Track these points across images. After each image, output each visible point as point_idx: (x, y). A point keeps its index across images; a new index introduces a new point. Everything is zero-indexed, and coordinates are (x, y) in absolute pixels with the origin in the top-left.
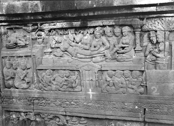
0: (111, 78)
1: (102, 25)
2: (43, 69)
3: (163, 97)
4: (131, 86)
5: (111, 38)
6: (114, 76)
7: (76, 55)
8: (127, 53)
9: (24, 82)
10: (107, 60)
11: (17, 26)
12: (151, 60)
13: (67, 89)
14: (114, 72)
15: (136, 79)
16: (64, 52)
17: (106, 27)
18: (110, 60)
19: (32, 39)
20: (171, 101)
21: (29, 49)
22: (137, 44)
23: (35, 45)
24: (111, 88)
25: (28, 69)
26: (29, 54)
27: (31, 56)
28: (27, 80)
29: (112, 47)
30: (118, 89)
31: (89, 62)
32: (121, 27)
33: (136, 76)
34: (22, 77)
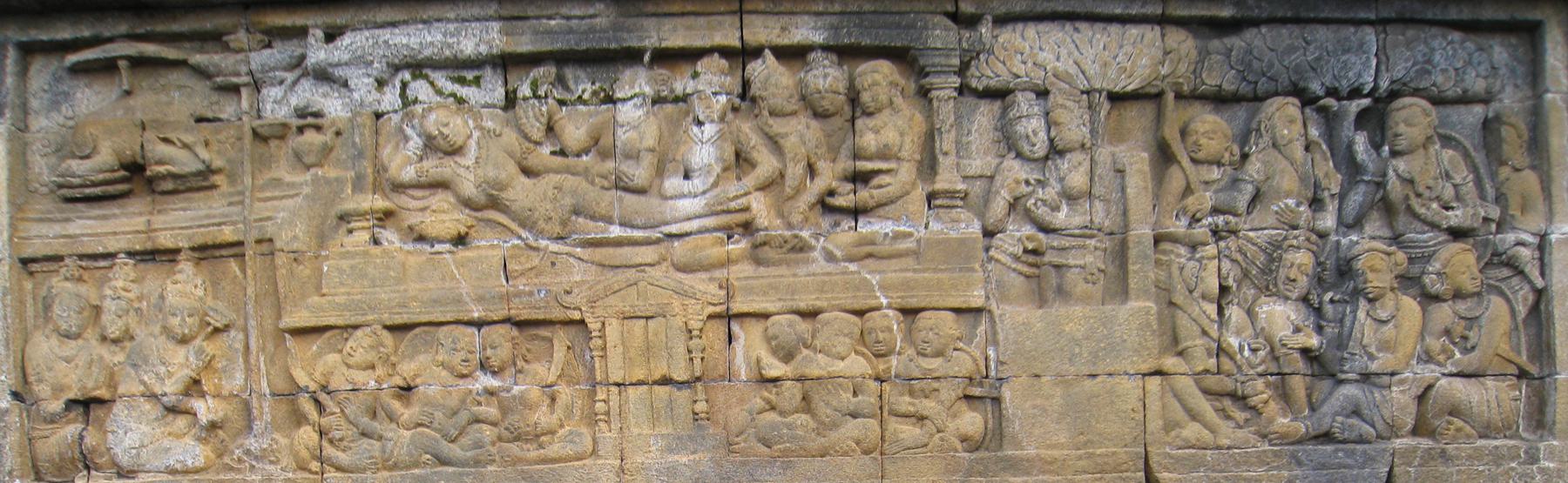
0: (788, 357)
1: (737, 43)
2: (332, 321)
3: (1090, 456)
4: (913, 404)
5: (793, 121)
6: (805, 352)
7: (564, 223)
8: (887, 208)
9: (181, 422)
10: (767, 252)
11: (150, 49)
12: (1019, 250)
13: (493, 450)
14: (803, 326)
15: (939, 360)
16: (479, 215)
17: (760, 61)
18: (784, 250)
19: (255, 133)
20: (1128, 474)
21: (224, 202)
22: (941, 158)
23: (268, 175)
24: (789, 419)
25: (217, 330)
26: (228, 234)
27: (240, 244)
28: (204, 409)
29: (795, 171)
30: (835, 426)
31: (647, 268)
32: (845, 67)
33: (937, 344)
34: (170, 388)
